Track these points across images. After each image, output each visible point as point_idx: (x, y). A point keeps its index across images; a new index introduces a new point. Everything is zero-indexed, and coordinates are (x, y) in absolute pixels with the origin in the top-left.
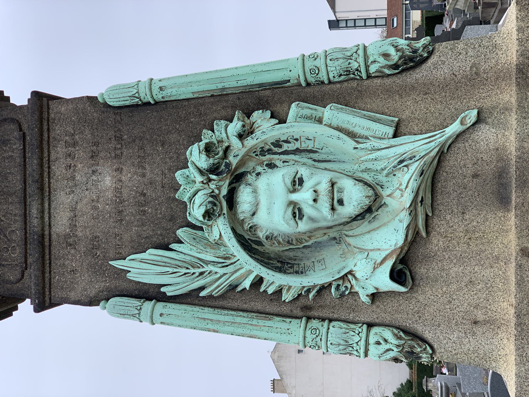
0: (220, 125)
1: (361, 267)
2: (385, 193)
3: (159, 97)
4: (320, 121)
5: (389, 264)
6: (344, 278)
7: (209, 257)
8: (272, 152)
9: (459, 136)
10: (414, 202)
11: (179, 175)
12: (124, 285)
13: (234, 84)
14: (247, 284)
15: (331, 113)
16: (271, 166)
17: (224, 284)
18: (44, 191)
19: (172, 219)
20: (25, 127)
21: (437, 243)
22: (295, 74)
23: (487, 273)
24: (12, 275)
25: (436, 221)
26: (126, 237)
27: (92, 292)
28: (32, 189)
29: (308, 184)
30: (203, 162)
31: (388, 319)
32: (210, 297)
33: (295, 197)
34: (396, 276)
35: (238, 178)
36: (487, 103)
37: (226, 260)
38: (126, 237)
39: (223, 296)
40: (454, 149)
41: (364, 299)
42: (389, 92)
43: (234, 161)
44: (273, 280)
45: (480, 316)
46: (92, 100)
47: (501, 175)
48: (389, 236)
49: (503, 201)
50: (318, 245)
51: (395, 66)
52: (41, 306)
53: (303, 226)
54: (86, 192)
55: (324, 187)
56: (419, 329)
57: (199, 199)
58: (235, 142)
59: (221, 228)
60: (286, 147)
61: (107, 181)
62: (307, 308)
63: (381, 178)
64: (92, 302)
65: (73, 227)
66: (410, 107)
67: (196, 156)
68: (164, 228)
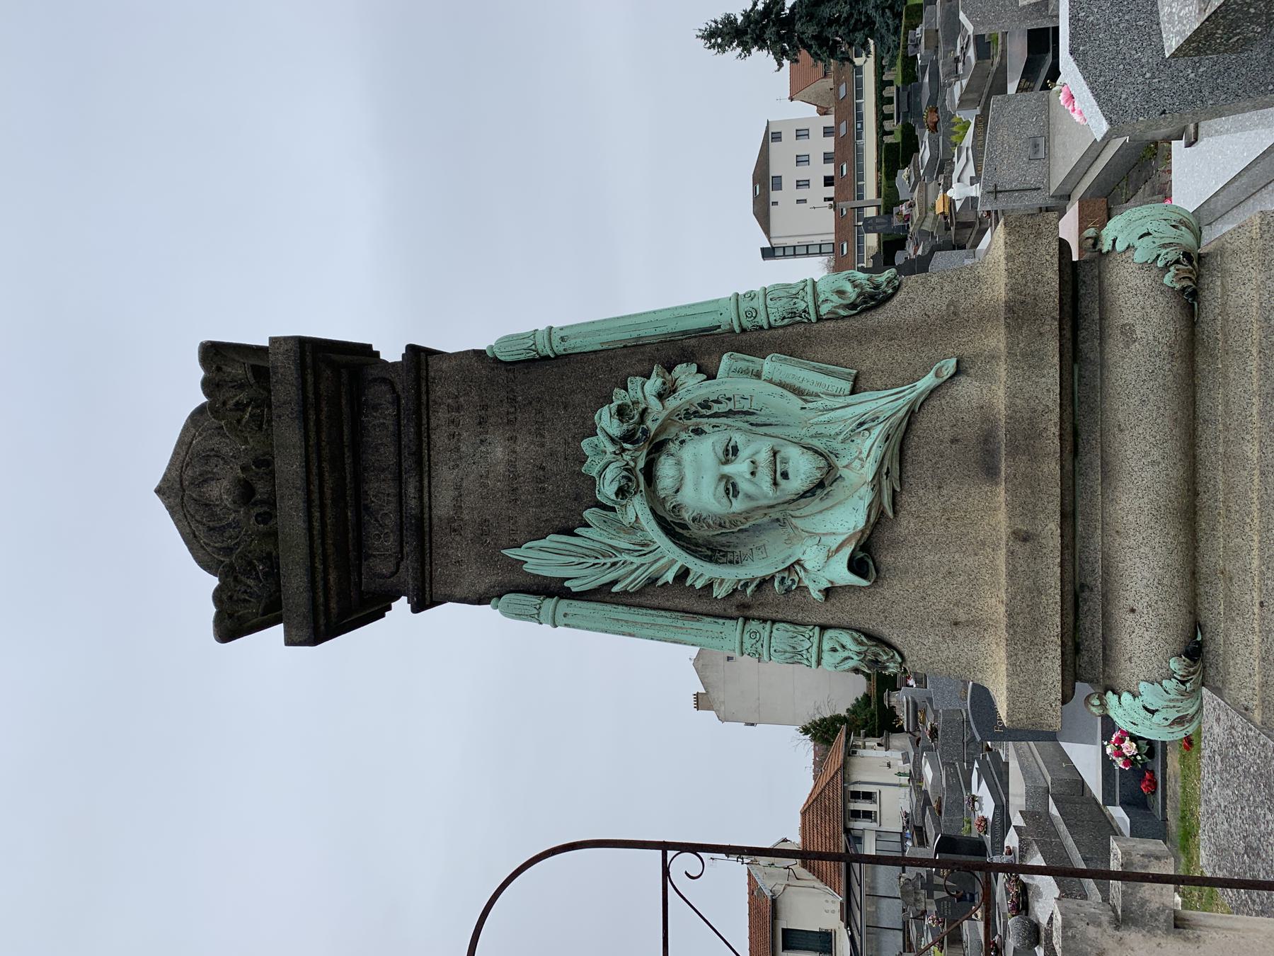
0: (634, 383)
1: (812, 556)
2: (840, 463)
3: (560, 349)
4: (758, 375)
5: (847, 551)
6: (790, 569)
7: (623, 544)
8: (699, 416)
9: (933, 391)
10: (878, 474)
11: (585, 444)
12: (520, 579)
13: (652, 332)
14: (669, 576)
15: (771, 365)
16: (698, 432)
17: (641, 576)
19: (577, 498)
20: (399, 388)
21: (906, 525)
22: (727, 318)
23: (971, 561)
24: (384, 568)
25: (905, 498)
26: (522, 520)
27: (481, 588)
28: (408, 463)
29: (744, 453)
30: (616, 428)
31: (845, 619)
32: (625, 592)
33: (728, 469)
34: (856, 566)
35: (658, 447)
36: (968, 351)
37: (644, 547)
38: (522, 520)
40: (927, 408)
42: (845, 337)
43: (652, 427)
44: (702, 571)
45: (962, 616)
46: (479, 354)
47: (987, 439)
48: (846, 517)
49: (991, 472)
50: (757, 529)
51: (853, 306)
52: (419, 606)
53: (738, 505)
54: (472, 466)
55: (764, 457)
56: (885, 632)
57: (610, 473)
58: (654, 403)
59: (637, 508)
60: (716, 408)
61: (499, 452)
62: (744, 606)
63: (836, 444)
64: (481, 600)
66: (870, 357)
67: (607, 421)
68: (568, 506)
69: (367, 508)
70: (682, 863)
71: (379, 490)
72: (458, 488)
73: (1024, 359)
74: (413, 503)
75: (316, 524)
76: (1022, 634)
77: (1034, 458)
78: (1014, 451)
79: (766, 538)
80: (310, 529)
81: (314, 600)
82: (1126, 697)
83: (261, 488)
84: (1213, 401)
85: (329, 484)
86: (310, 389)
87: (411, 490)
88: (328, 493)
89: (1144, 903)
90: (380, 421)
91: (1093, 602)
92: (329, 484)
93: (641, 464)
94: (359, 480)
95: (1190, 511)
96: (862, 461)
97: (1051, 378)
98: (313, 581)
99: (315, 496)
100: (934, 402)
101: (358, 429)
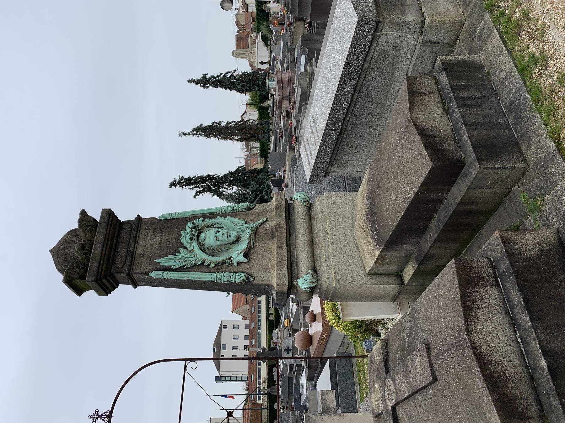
1: (234, 255)
6: (229, 259)
7: (189, 256)
8: (210, 227)
9: (262, 224)
10: (250, 237)
12: (158, 267)
13: (201, 212)
18: (136, 241)
21: (256, 250)
22: (219, 210)
23: (269, 256)
24: (119, 266)
26: (162, 253)
28: (132, 239)
31: (241, 270)
32: (187, 268)
34: (245, 256)
35: (200, 233)
36: (269, 217)
39: (191, 268)
40: (261, 227)
41: (235, 264)
42: (244, 215)
44: (209, 259)
45: (267, 267)
48: (243, 246)
51: (246, 209)
59: (195, 244)
60: (215, 226)
61: (158, 239)
63: (241, 233)
65: (144, 251)
66: (249, 218)
69: (117, 252)
70: (191, 365)
71: (122, 248)
72: (145, 247)
73: (279, 215)
74: (132, 249)
75: (104, 252)
76: (279, 265)
77: (281, 233)
78: (277, 231)
79: (224, 253)
80: (102, 253)
81: (98, 270)
82: (301, 278)
83: (87, 247)
84: (315, 227)
85: (102, 255)
86: (110, 221)
87: (132, 246)
88: (108, 245)
89: (328, 405)
90: (125, 236)
91: (294, 264)
92: (102, 255)
93: (196, 234)
94: (116, 245)
95: (312, 244)
96: (246, 237)
97: (284, 218)
98: (99, 266)
99: (105, 246)
100: (262, 226)
101: (119, 233)
